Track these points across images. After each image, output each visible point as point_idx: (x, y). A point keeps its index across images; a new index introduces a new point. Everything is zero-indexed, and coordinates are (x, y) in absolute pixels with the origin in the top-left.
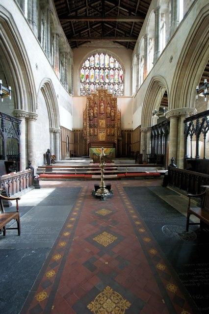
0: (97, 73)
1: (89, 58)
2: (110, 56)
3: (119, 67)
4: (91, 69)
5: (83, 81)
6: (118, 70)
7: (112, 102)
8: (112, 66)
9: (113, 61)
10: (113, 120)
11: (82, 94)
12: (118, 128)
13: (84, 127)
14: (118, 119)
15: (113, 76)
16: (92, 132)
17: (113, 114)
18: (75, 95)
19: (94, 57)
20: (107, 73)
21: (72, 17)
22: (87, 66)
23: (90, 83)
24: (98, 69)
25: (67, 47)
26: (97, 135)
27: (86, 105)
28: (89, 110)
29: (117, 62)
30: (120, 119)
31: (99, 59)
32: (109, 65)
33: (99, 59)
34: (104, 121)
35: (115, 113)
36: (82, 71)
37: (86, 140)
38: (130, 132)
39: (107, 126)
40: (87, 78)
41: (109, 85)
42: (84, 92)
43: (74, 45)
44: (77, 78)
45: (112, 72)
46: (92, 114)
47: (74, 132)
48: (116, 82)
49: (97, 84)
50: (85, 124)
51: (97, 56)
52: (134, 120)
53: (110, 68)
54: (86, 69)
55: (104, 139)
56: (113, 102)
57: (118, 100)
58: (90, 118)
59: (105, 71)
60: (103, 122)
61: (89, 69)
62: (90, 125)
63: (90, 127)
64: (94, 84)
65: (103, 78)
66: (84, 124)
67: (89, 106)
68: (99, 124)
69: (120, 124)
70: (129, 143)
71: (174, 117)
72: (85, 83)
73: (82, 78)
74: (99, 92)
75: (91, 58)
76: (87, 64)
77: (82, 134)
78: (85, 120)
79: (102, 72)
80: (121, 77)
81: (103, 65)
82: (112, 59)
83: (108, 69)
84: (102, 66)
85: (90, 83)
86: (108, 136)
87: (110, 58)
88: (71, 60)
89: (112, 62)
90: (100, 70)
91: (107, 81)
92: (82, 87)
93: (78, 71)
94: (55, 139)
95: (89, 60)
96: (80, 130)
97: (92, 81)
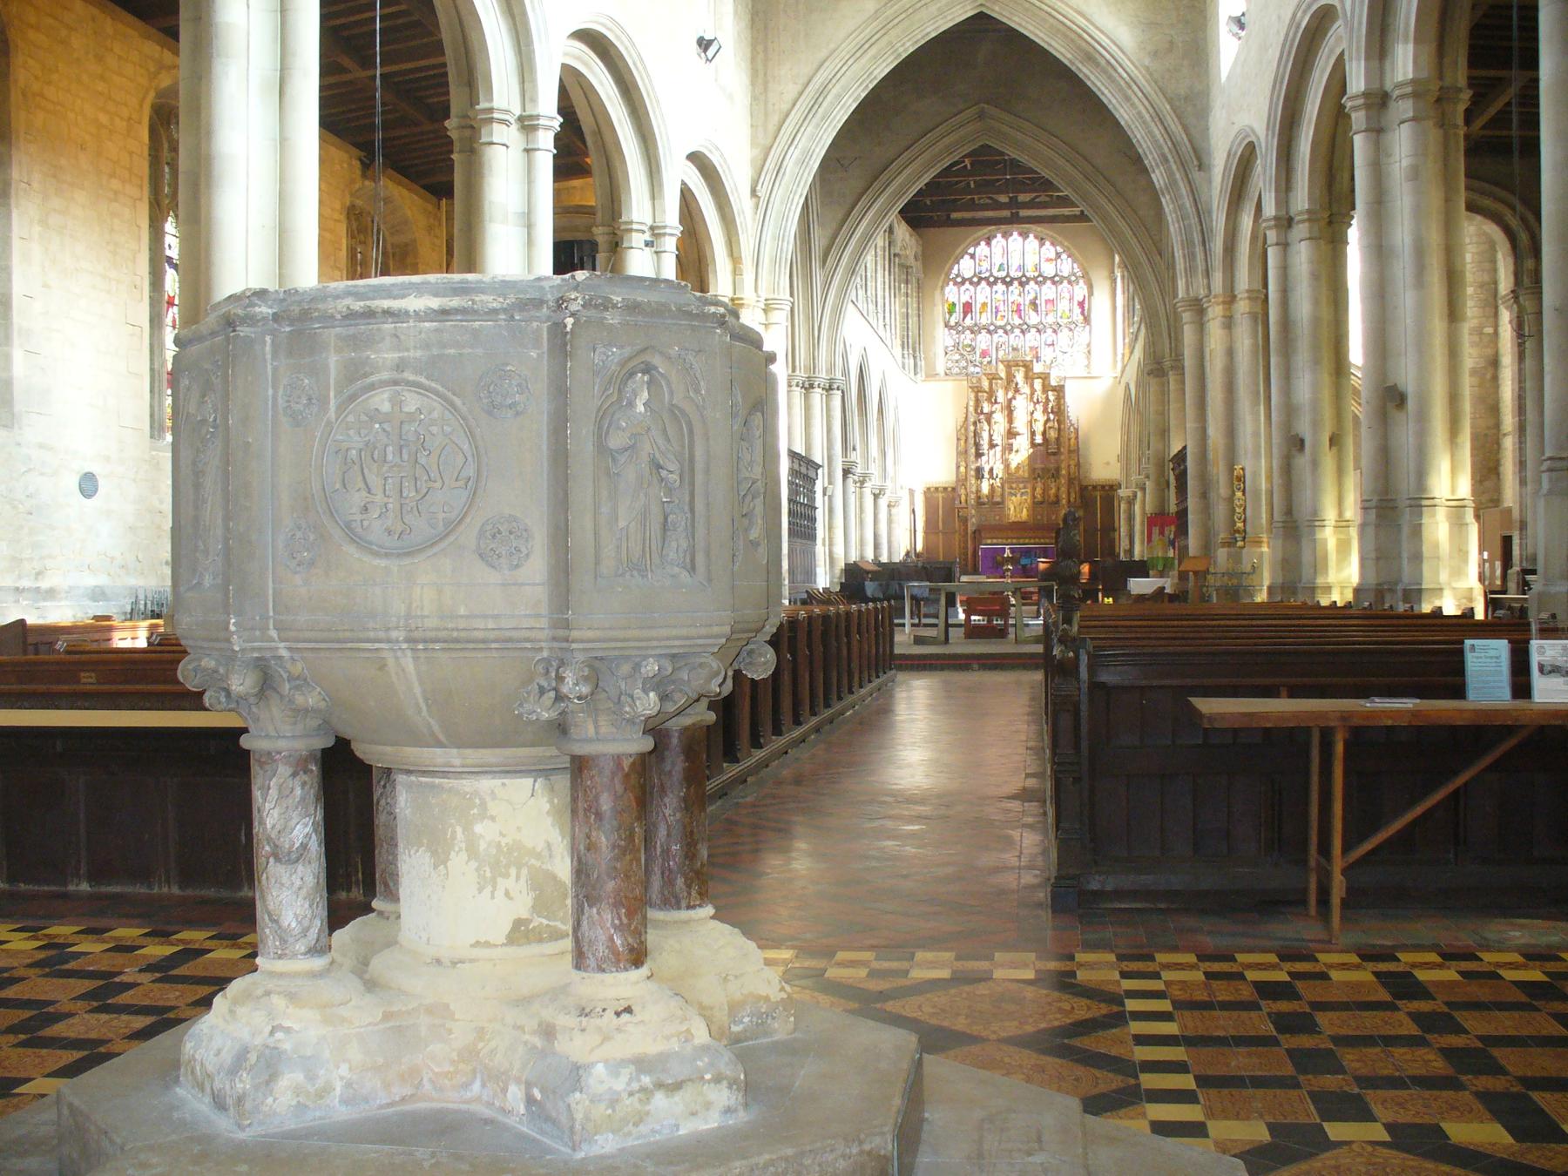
0: (999, 296)
1: (971, 250)
2: (1042, 240)
3: (1074, 274)
4: (978, 283)
5: (952, 323)
6: (1070, 282)
8: (1048, 270)
9: (1053, 255)
10: (1054, 454)
11: (950, 364)
12: (1071, 481)
13: (958, 480)
14: (1070, 451)
18: (931, 375)
19: (988, 244)
20: (1032, 296)
22: (968, 274)
24: (1004, 281)
26: (1002, 502)
27: (967, 408)
28: (975, 424)
29: (1064, 256)
30: (1075, 451)
31: (1006, 252)
32: (1037, 268)
33: (1006, 252)
35: (1059, 429)
36: (952, 293)
37: (964, 521)
38: (1109, 490)
40: (966, 312)
41: (1039, 331)
42: (957, 357)
45: (1048, 291)
48: (1063, 321)
49: (1001, 332)
50: (962, 469)
51: (998, 241)
53: (1041, 280)
54: (963, 283)
55: (1024, 515)
59: (1027, 287)
61: (971, 283)
65: (1018, 311)
66: (958, 467)
67: (976, 410)
69: (1078, 465)
70: (1110, 527)
73: (951, 313)
74: (1009, 365)
75: (979, 250)
76: (966, 267)
77: (954, 499)
79: (1016, 292)
80: (1081, 304)
81: (1019, 268)
82: (1049, 250)
83: (1035, 279)
84: (1014, 274)
85: (975, 330)
86: (1036, 504)
87: (1042, 245)
88: (916, 266)
89: (1049, 260)
90: (1008, 284)
91: (1033, 319)
92: (950, 342)
93: (937, 293)
95: (973, 256)
96: (945, 489)
97: (985, 319)
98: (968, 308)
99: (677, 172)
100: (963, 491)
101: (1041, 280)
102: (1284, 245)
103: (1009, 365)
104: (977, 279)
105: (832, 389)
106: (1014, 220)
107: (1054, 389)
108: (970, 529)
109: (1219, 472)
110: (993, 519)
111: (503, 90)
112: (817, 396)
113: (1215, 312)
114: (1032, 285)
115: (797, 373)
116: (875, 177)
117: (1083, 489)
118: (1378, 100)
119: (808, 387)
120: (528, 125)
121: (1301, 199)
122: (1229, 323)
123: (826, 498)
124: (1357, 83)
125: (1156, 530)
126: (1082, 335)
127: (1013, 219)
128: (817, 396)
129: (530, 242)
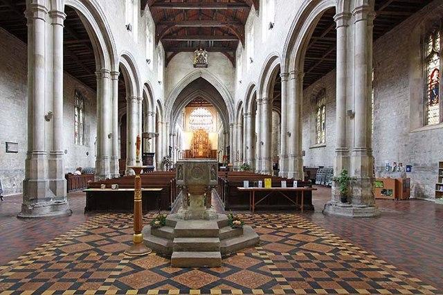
44: (188, 121)
52: (215, 146)
58: (195, 145)
60: (201, 146)
76: (193, 114)
82: (206, 111)
85: (194, 124)
91: (204, 122)
97: (196, 122)
99: (156, 104)
102: (246, 118)
103: (200, 130)
109: (235, 150)
111: (135, 94)
113: (235, 126)
116: (182, 102)
117: (211, 151)
118: (261, 100)
120: (138, 99)
121: (249, 111)
122: (237, 128)
124: (258, 97)
126: (212, 125)
127: (201, 105)
129: (139, 117)
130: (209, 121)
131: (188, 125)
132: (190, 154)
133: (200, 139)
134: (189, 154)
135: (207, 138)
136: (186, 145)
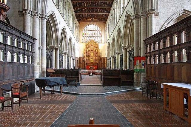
7: (97, 46)
12: (99, 57)
15: (97, 33)
16: (87, 58)
17: (97, 51)
20: (94, 33)
21: (81, 17)
23: (87, 37)
25: (78, 25)
30: (100, 53)
34: (93, 54)
36: (83, 32)
37: (85, 62)
38: (104, 58)
39: (94, 56)
43: (79, 21)
46: (88, 51)
47: (80, 58)
51: (90, 25)
52: (104, 54)
53: (95, 31)
56: (97, 45)
57: (99, 45)
58: (87, 53)
60: (92, 54)
62: (86, 55)
63: (87, 56)
64: (89, 37)
68: (90, 55)
69: (100, 55)
70: (104, 63)
71: (112, 57)
72: (84, 37)
74: (91, 41)
76: (85, 28)
78: (84, 53)
82: (97, 27)
84: (92, 30)
85: (87, 37)
91: (94, 36)
92: (83, 38)
94: (74, 62)
97: (88, 36)
98: (86, 34)
100: (84, 58)
101: (95, 31)
103: (91, 41)
104: (87, 30)
105: (43, 18)
106: (92, 21)
107: (97, 45)
108: (86, 63)
110: (89, 62)
112: (37, 19)
114: (94, 31)
115: (29, 9)
119: (34, 15)
123: (40, 50)
125: (138, 62)
128: (37, 19)
130: (99, 35)
131: (81, 38)
132: (83, 61)
133: (91, 48)
134: (81, 60)
135: (97, 48)
136: (79, 51)
